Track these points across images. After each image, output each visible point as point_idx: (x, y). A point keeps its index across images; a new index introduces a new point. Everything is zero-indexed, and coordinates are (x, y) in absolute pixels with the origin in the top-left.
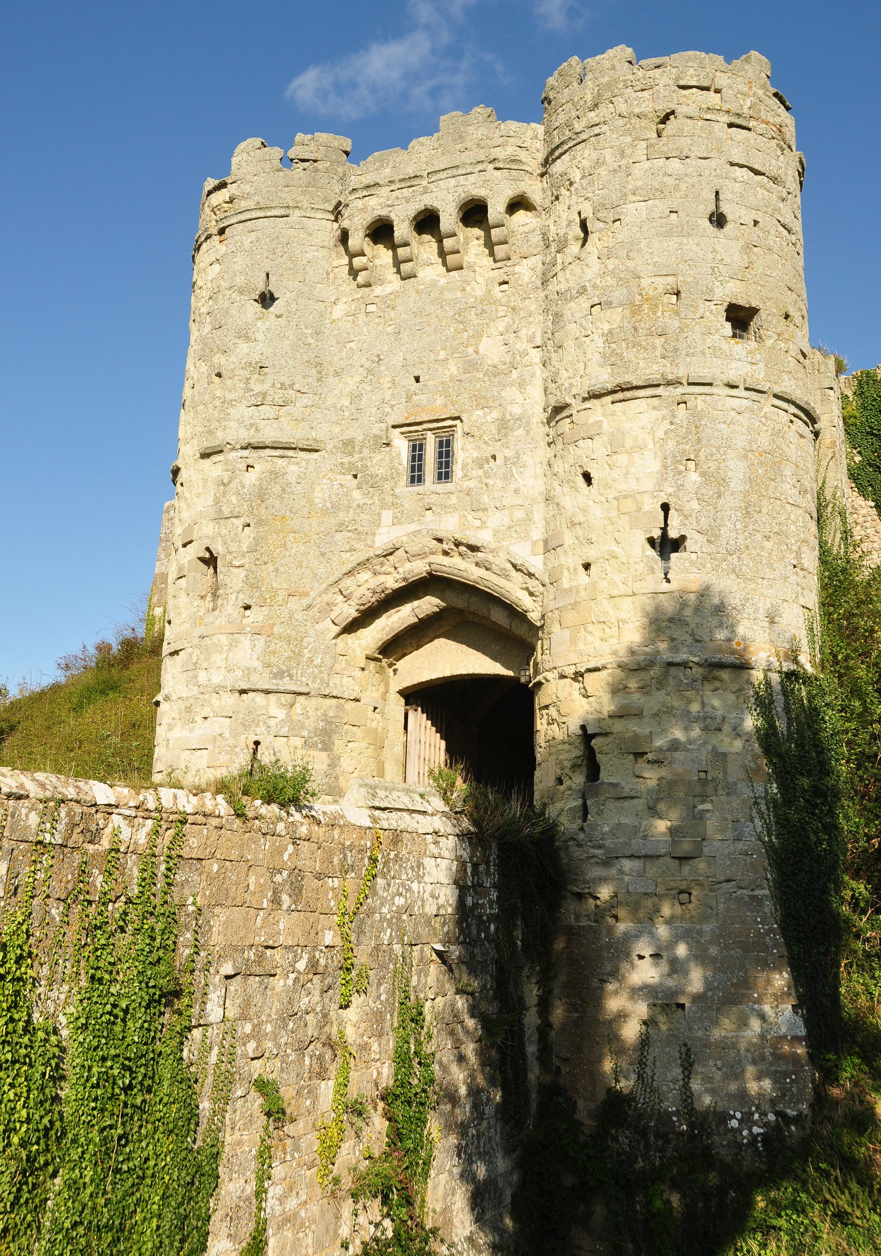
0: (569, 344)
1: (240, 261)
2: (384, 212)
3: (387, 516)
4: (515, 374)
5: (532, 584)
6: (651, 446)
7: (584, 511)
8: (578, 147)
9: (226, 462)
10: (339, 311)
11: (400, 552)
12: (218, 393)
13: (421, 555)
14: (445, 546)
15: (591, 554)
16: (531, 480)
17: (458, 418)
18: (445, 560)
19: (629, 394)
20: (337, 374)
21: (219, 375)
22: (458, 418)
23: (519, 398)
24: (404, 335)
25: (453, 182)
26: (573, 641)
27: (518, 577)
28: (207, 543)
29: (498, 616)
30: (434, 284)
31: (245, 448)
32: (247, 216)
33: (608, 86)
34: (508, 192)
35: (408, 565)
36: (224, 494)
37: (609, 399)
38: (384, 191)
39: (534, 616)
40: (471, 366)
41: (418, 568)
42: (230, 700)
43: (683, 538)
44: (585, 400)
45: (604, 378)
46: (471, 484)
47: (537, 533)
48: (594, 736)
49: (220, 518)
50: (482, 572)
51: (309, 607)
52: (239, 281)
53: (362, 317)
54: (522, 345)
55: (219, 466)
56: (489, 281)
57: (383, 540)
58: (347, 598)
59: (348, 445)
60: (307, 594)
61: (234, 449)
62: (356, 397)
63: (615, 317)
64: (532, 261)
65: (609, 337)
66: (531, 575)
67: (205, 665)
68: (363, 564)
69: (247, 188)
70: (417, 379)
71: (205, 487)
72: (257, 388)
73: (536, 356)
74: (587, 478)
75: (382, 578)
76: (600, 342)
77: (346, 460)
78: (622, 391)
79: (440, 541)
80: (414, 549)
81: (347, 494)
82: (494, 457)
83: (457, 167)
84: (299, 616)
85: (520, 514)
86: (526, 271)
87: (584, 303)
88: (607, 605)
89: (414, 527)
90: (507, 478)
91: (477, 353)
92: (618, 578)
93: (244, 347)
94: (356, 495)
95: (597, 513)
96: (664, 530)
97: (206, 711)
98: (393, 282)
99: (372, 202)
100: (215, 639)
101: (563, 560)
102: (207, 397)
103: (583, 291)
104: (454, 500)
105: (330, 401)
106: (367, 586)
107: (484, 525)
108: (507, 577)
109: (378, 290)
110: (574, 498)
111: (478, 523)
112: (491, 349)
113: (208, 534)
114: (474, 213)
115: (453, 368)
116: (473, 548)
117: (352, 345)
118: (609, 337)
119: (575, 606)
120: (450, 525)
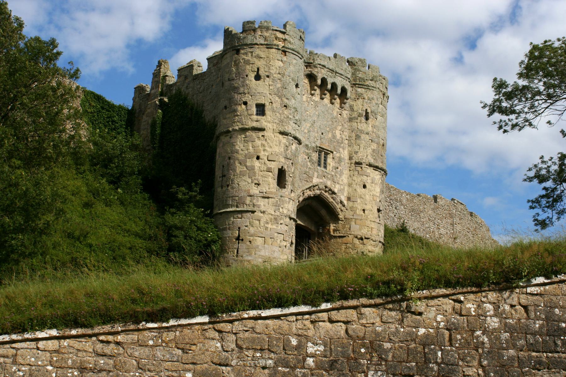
0: (362, 146)
1: (292, 68)
2: (326, 77)
4: (342, 145)
5: (343, 208)
7: (365, 195)
9: (288, 139)
10: (304, 98)
11: (317, 187)
12: (285, 112)
14: (327, 189)
15: (366, 207)
16: (345, 179)
20: (304, 121)
21: (285, 106)
22: (332, 152)
24: (320, 117)
26: (360, 230)
27: (340, 205)
28: (281, 164)
30: (326, 105)
31: (293, 137)
32: (294, 53)
33: (376, 77)
36: (287, 150)
38: (326, 69)
39: (341, 216)
40: (334, 136)
42: (288, 220)
44: (367, 165)
45: (372, 161)
46: (333, 173)
47: (346, 194)
49: (286, 158)
50: (331, 200)
52: (292, 75)
54: (343, 137)
55: (285, 139)
57: (315, 181)
61: (291, 136)
62: (309, 131)
63: (374, 146)
64: (346, 112)
65: (374, 151)
66: (344, 206)
67: (282, 206)
69: (291, 40)
70: (322, 134)
71: (280, 144)
72: (297, 118)
73: (346, 142)
74: (365, 187)
76: (371, 150)
78: (376, 168)
79: (326, 187)
80: (321, 187)
81: (306, 162)
82: (338, 168)
83: (342, 75)
85: (342, 187)
86: (346, 113)
87: (367, 137)
88: (369, 222)
89: (321, 181)
90: (341, 176)
92: (372, 216)
93: (293, 101)
94: (309, 164)
95: (367, 197)
97: (282, 222)
98: (317, 98)
99: (323, 71)
100: (286, 198)
101: (357, 206)
102: (281, 112)
103: (368, 134)
105: (302, 129)
107: (335, 187)
108: (338, 204)
109: (314, 98)
110: (360, 190)
113: (281, 162)
115: (330, 135)
116: (334, 193)
118: (374, 151)
119: (361, 220)
120: (329, 183)
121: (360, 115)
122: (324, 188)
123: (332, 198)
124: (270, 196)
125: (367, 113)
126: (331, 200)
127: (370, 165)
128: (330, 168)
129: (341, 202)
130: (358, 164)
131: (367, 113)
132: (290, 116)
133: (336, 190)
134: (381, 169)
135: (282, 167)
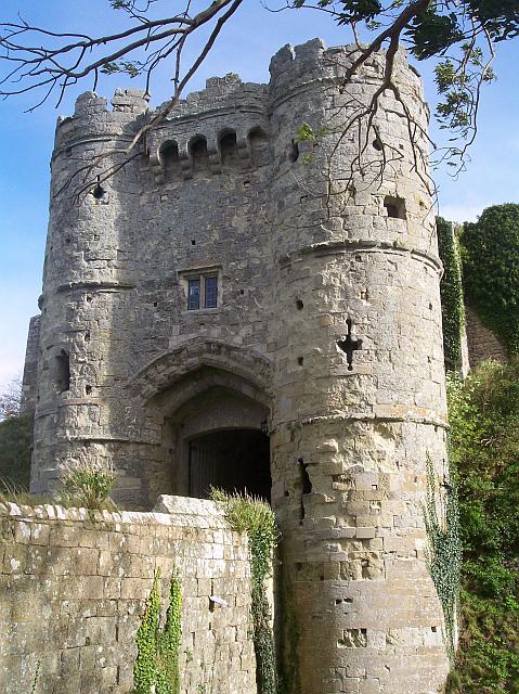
3: (176, 329)
6: (338, 285)
8: (292, 99)
10: (144, 200)
13: (200, 353)
15: (305, 351)
17: (220, 267)
18: (215, 357)
19: (325, 253)
23: (258, 254)
25: (214, 120)
29: (247, 391)
33: (308, 63)
34: (248, 126)
35: (190, 360)
37: (313, 255)
40: (226, 234)
41: (195, 360)
43: (360, 341)
46: (229, 308)
48: (307, 465)
51: (127, 387)
53: (158, 203)
56: (238, 182)
57: (174, 343)
58: (152, 381)
59: (150, 284)
60: (126, 379)
62: (156, 253)
68: (163, 360)
70: (194, 243)
74: (300, 305)
75: (174, 368)
77: (149, 294)
79: (209, 343)
82: (242, 292)
84: (123, 392)
89: (192, 336)
90: (251, 304)
91: (230, 226)
94: (156, 316)
96: (348, 336)
104: (218, 318)
106: (162, 374)
109: (169, 187)
111: (232, 333)
112: (239, 223)
114: (227, 138)
115: (216, 236)
116: (230, 349)
117: (153, 221)
121: (283, 160)
122: (205, 347)
123: (235, 359)
124: (44, 413)
125: (295, 147)
126: (233, 364)
127: (305, 252)
128: (220, 300)
129: (258, 360)
130: (285, 261)
131: (295, 147)
132: (76, 254)
133: (238, 341)
134: (339, 246)
135: (63, 351)
